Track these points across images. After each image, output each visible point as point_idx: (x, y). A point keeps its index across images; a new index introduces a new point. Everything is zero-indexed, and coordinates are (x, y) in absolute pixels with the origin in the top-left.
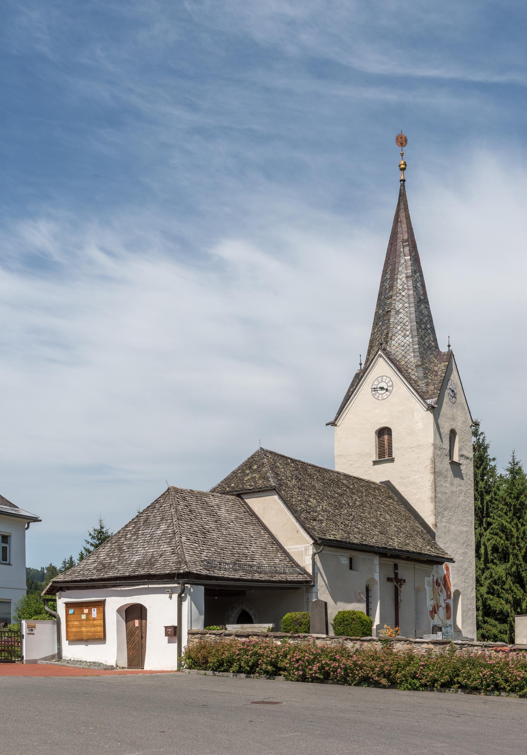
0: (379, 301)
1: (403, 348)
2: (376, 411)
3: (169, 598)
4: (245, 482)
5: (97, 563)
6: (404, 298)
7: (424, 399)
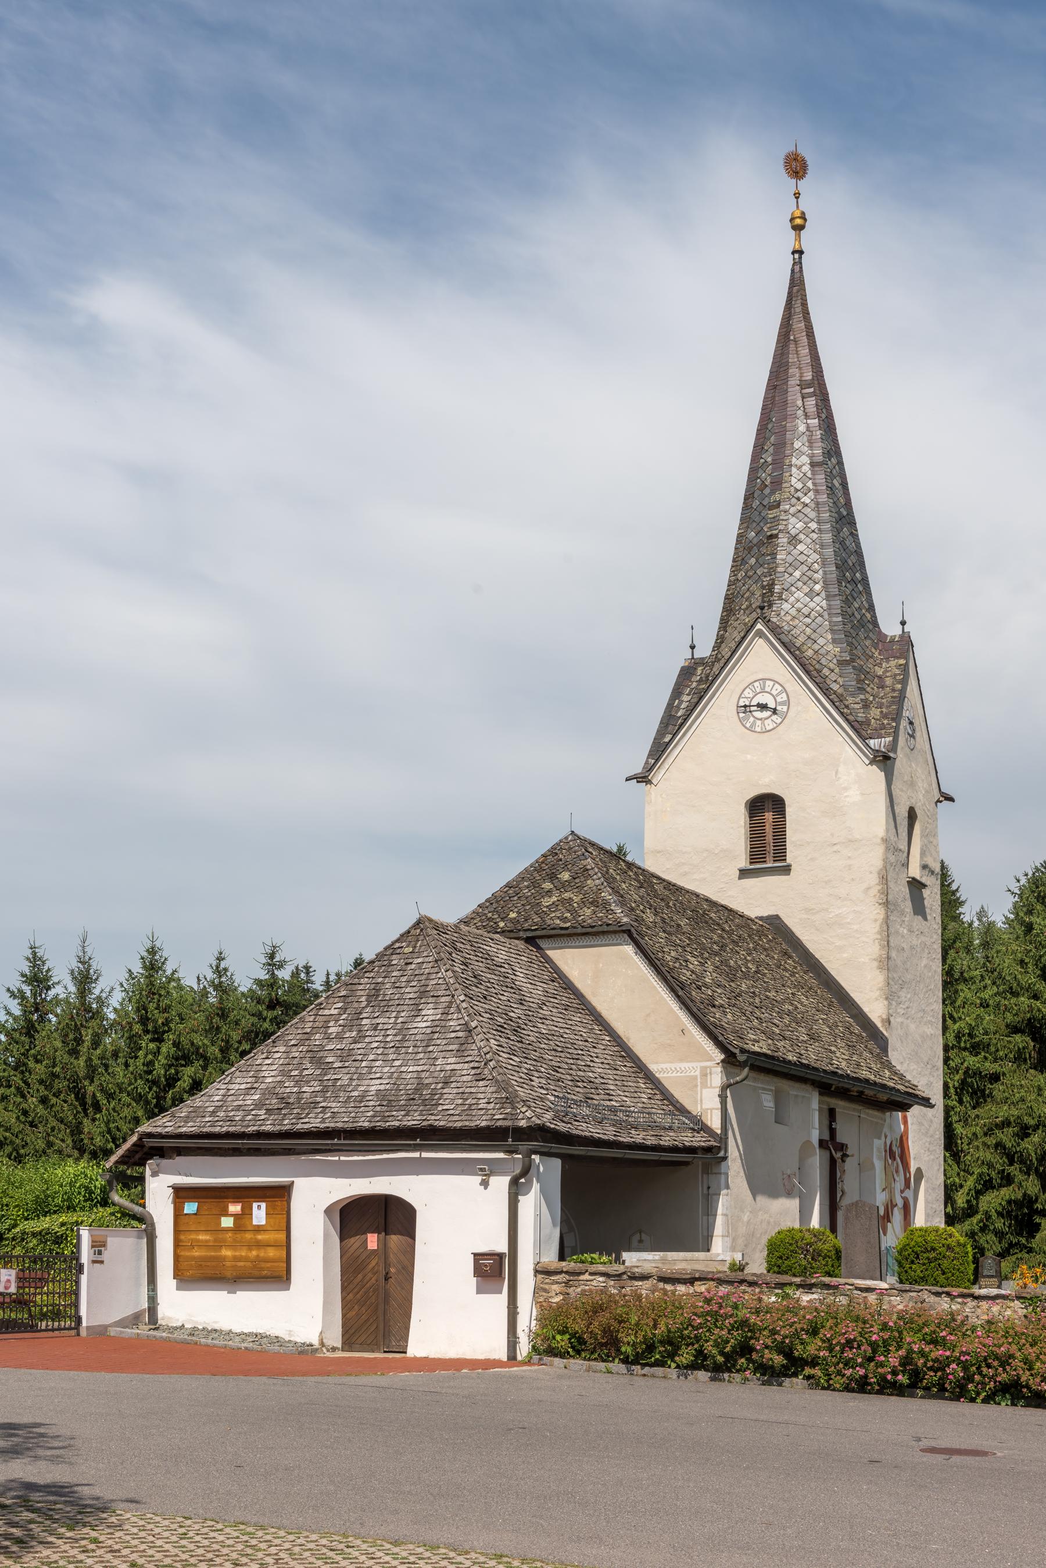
0: (746, 512)
1: (808, 620)
2: (749, 757)
3: (481, 1184)
4: (545, 909)
5: (258, 1091)
6: (807, 510)
7: (863, 739)
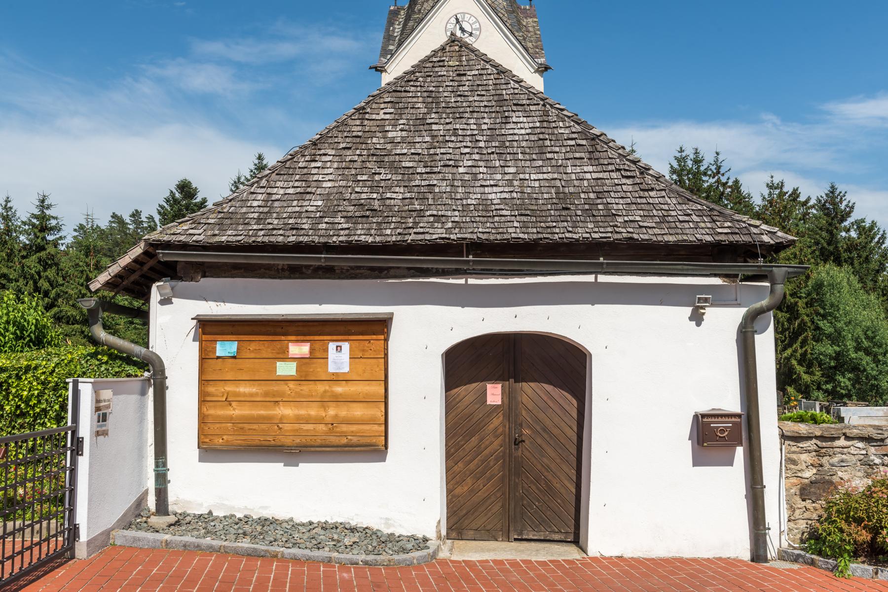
3: (691, 319)
